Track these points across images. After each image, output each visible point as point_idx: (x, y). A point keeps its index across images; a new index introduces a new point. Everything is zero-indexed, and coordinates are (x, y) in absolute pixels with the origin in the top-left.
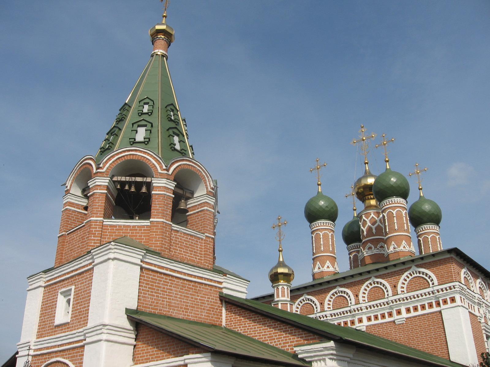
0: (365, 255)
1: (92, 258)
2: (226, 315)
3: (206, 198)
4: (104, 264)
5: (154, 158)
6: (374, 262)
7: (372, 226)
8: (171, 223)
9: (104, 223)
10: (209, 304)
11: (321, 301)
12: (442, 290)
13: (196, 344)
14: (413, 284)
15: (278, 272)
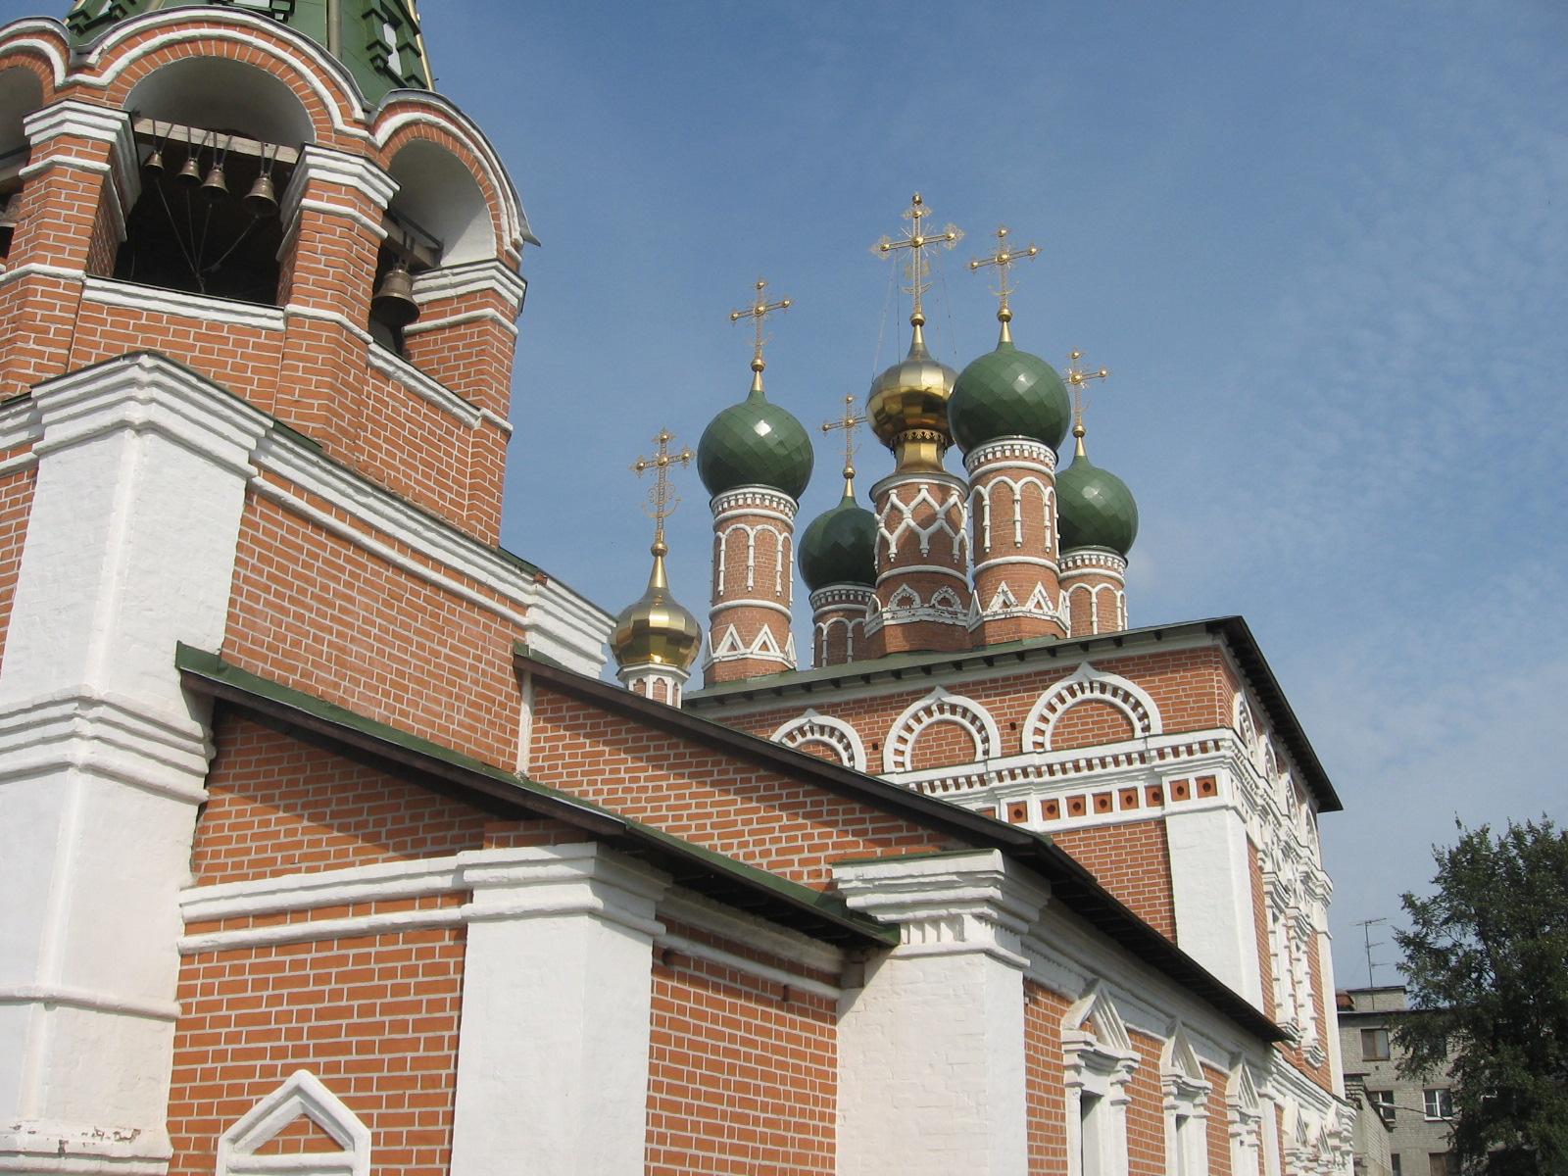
0: (886, 623)
1: (35, 423)
2: (534, 731)
3: (494, 272)
4: (96, 446)
5: (320, 71)
6: (915, 648)
7: (919, 529)
8: (370, 338)
9: (87, 294)
10: (476, 682)
12: (1176, 751)
13: (529, 804)
14: (1076, 725)
15: (651, 625)
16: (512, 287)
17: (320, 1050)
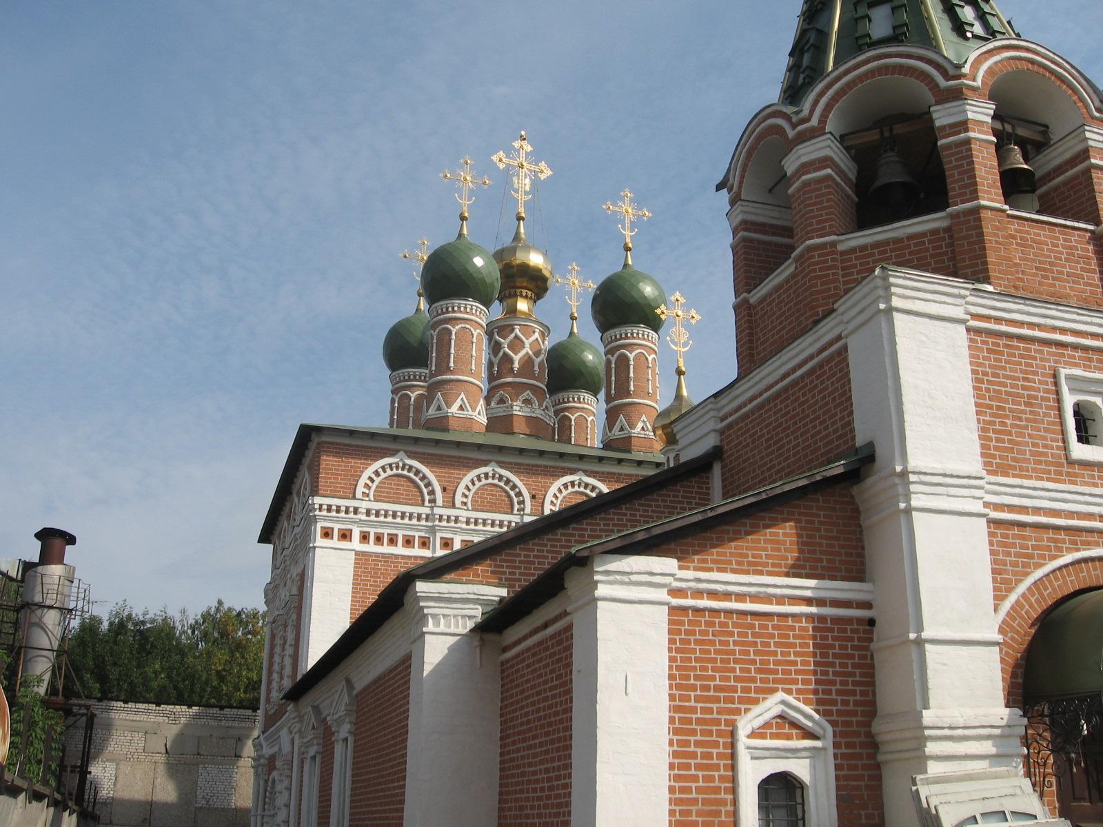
0: (514, 412)
6: (532, 434)
11: (533, 489)
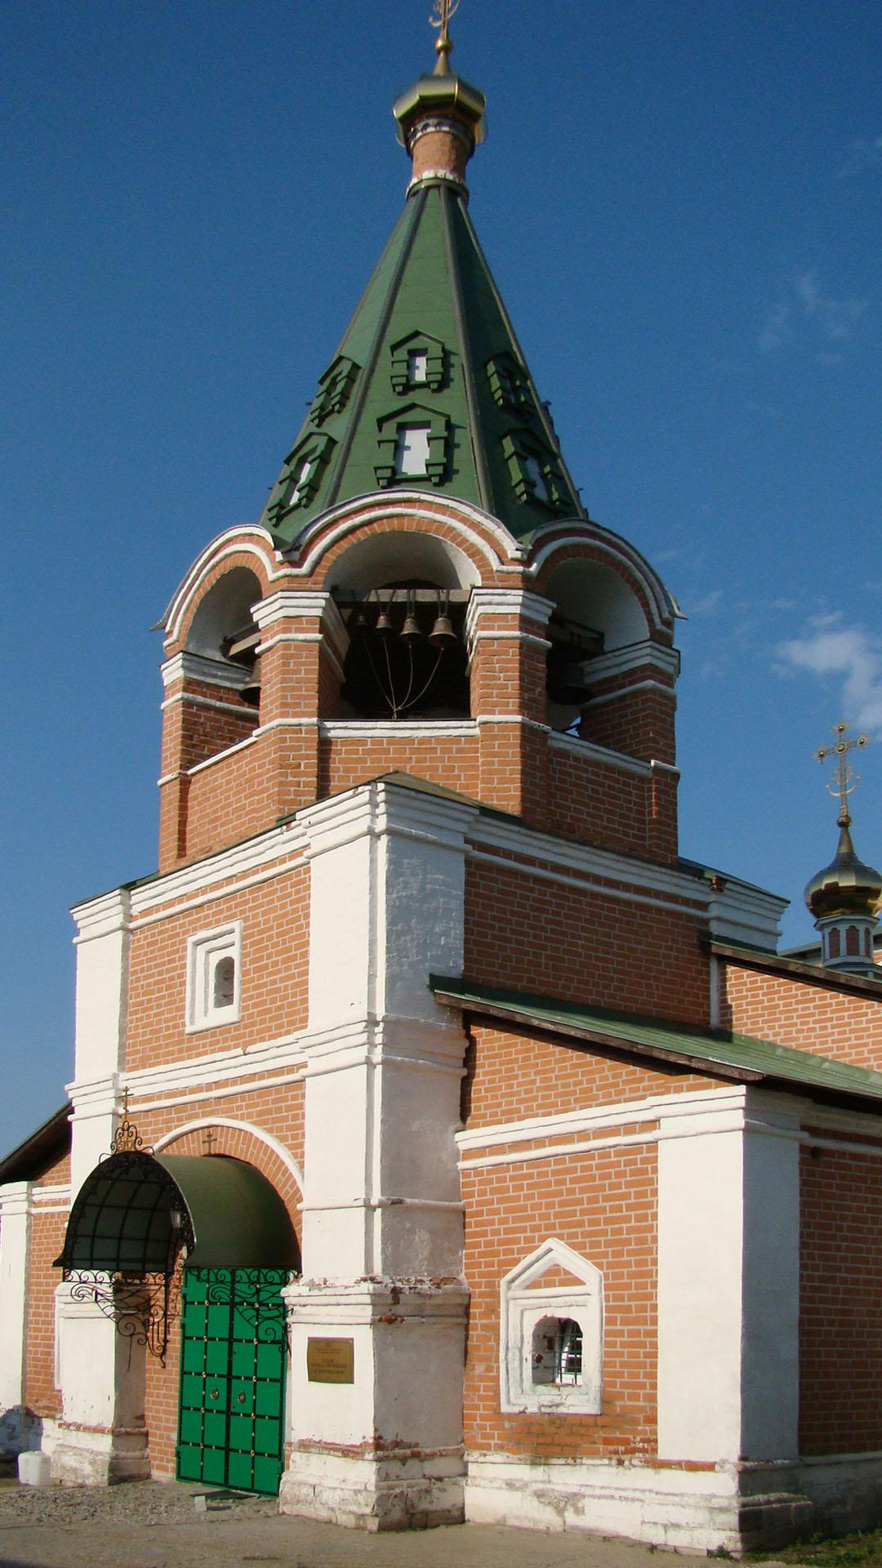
3: (649, 650)
16: (668, 659)
17: (563, 1226)
